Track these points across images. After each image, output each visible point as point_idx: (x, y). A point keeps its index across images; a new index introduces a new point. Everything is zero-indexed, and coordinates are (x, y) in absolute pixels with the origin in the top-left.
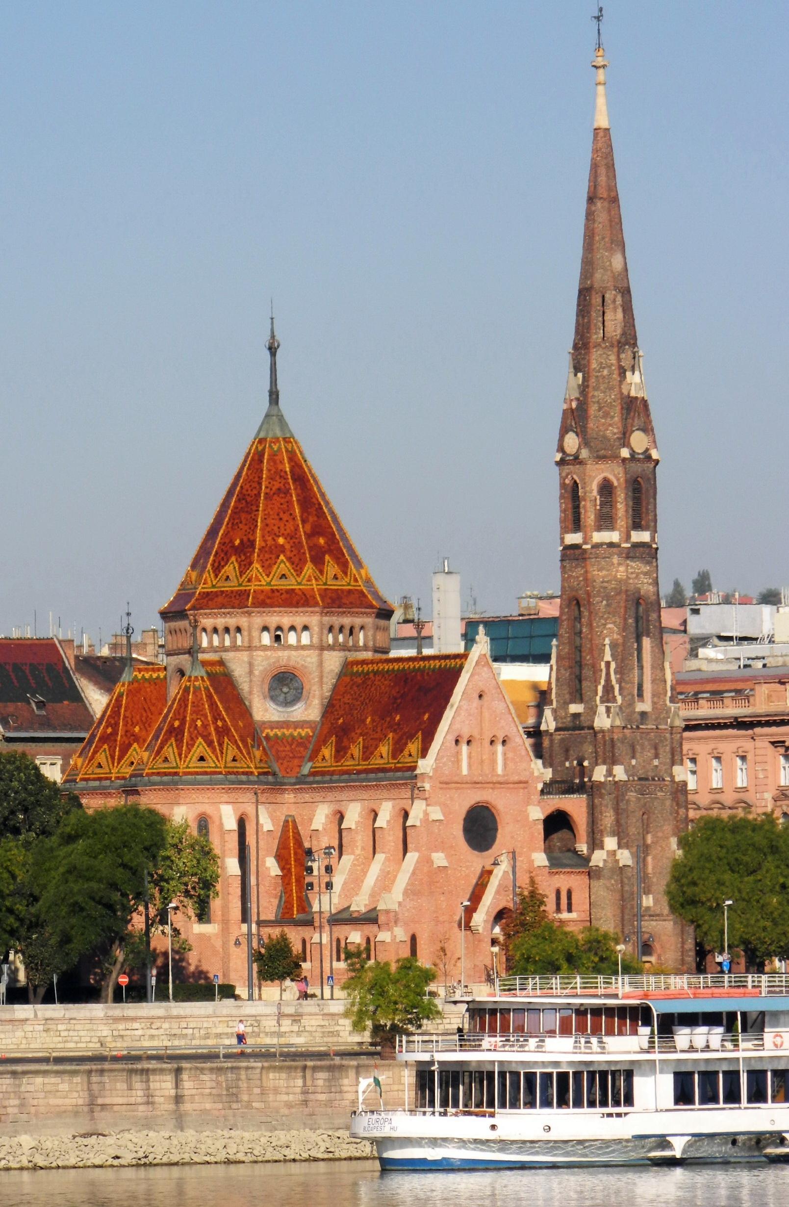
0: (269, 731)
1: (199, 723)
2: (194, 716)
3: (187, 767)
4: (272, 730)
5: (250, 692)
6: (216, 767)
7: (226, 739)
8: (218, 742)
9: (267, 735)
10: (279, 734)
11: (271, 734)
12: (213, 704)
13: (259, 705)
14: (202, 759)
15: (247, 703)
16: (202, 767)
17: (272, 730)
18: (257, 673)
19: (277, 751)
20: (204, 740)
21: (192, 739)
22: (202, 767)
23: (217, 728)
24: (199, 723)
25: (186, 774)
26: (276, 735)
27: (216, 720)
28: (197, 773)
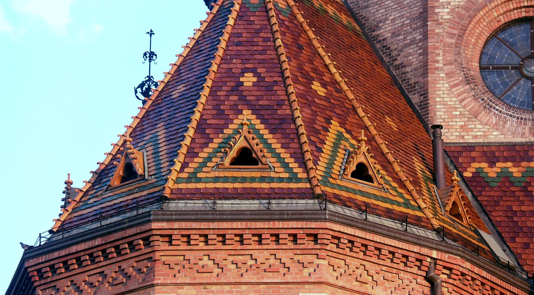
0: (484, 165)
1: (249, 80)
2: (236, 65)
3: (193, 177)
4: (492, 164)
5: (424, 69)
6: (294, 178)
7: (335, 126)
8: (310, 124)
9: (477, 174)
10: (515, 171)
11: (492, 172)
12: (297, 46)
13: (452, 101)
14: (246, 158)
15: (415, 99)
16: (244, 180)
17: (492, 164)
18: (444, 13)
19: (510, 213)
20: (259, 117)
21: (220, 114)
22: (244, 180)
23: (307, 98)
24: (249, 80)
25: (181, 195)
26: (505, 176)
27: (311, 80)
28: (225, 195)
